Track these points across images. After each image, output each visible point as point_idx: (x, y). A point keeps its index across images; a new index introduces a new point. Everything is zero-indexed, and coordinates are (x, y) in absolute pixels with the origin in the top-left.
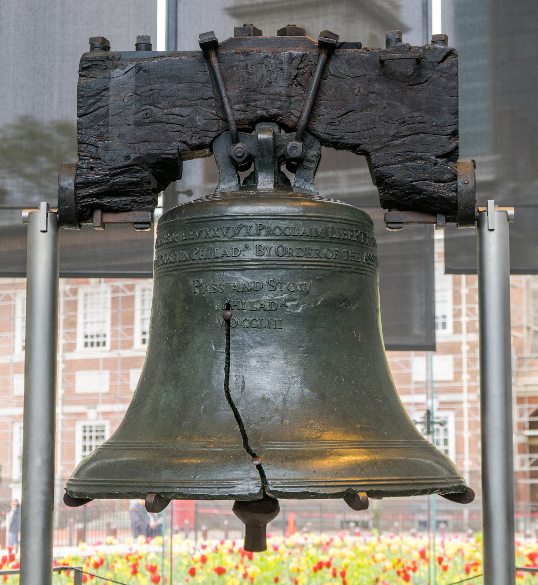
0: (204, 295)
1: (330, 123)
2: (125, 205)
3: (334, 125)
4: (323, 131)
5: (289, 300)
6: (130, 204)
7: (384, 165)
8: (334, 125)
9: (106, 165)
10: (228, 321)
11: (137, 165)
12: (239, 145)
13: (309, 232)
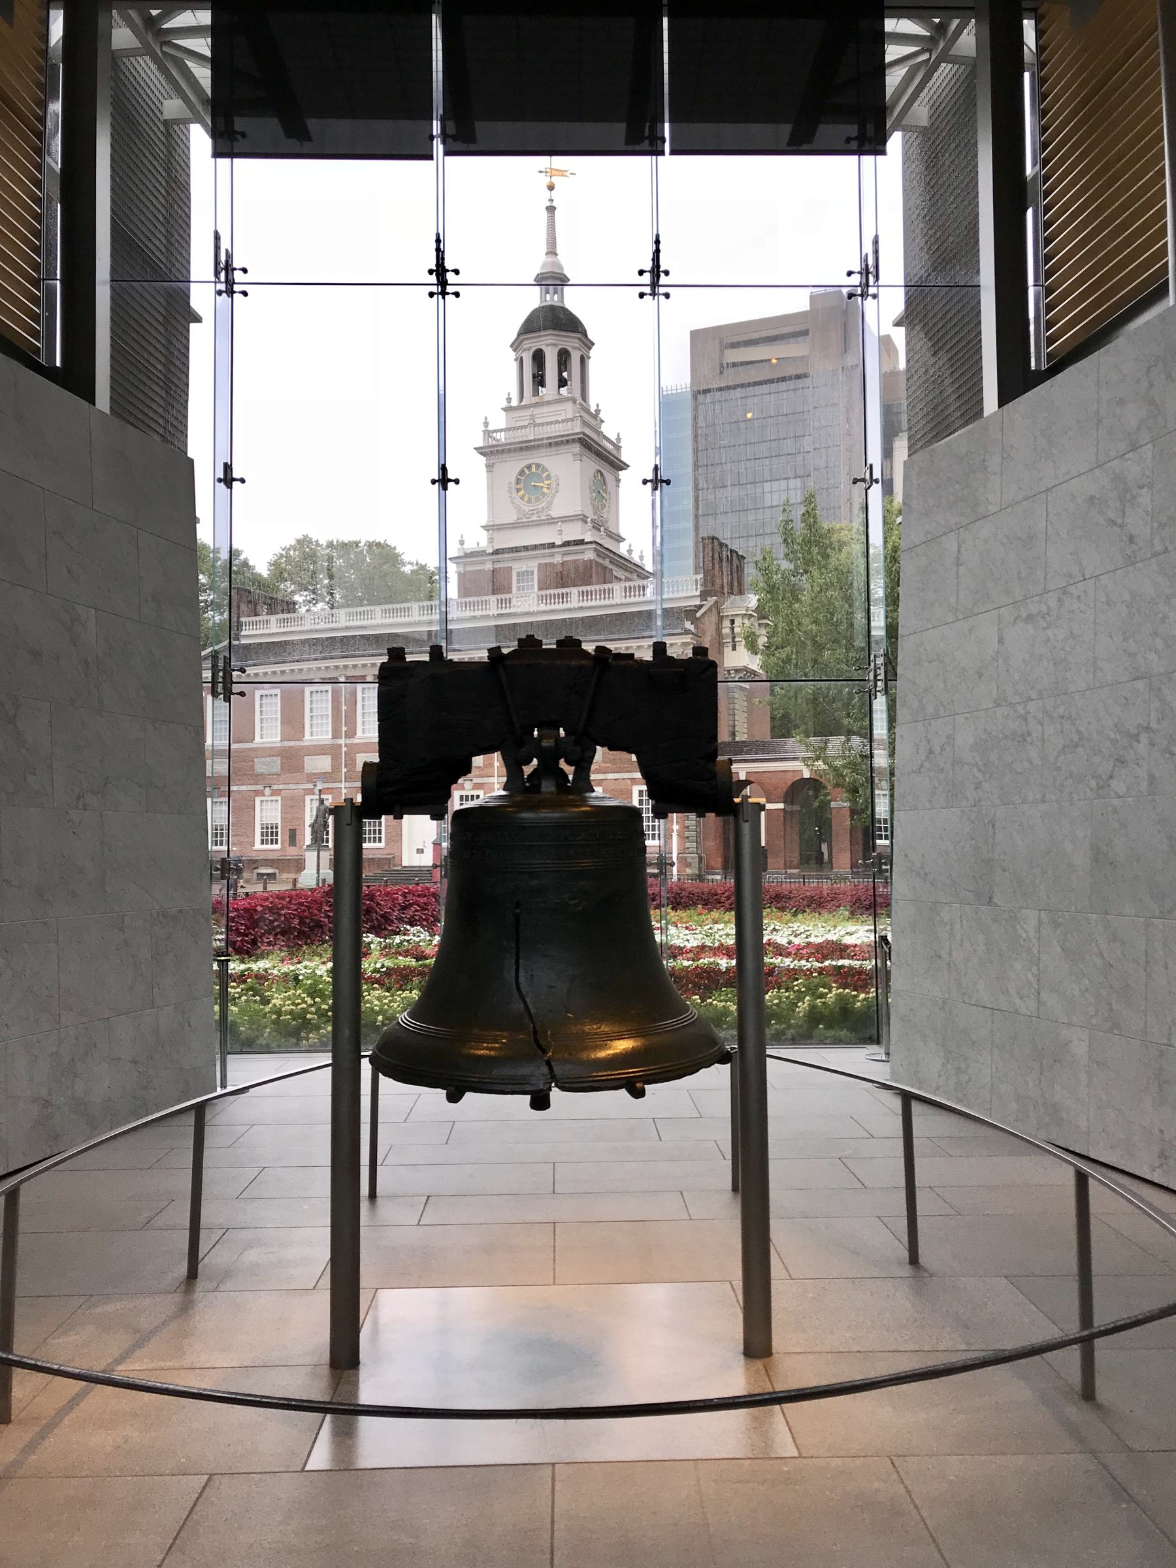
10: (517, 918)
12: (524, 749)
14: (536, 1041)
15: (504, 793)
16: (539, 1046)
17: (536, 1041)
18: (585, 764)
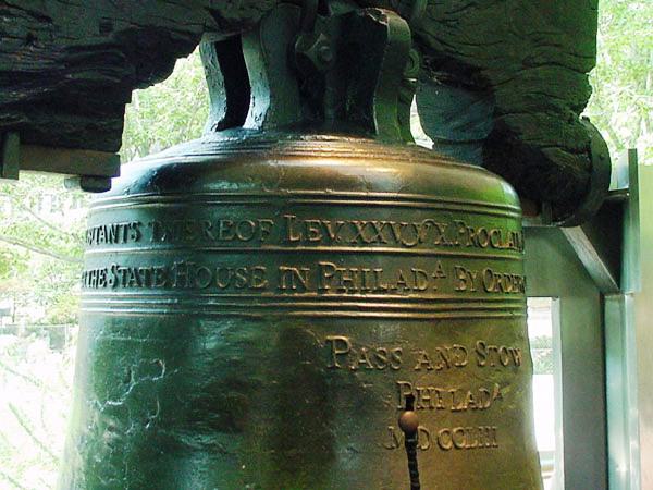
1: (443, 21)
3: (449, 26)
4: (435, 34)
8: (449, 26)
10: (411, 432)
12: (322, 37)
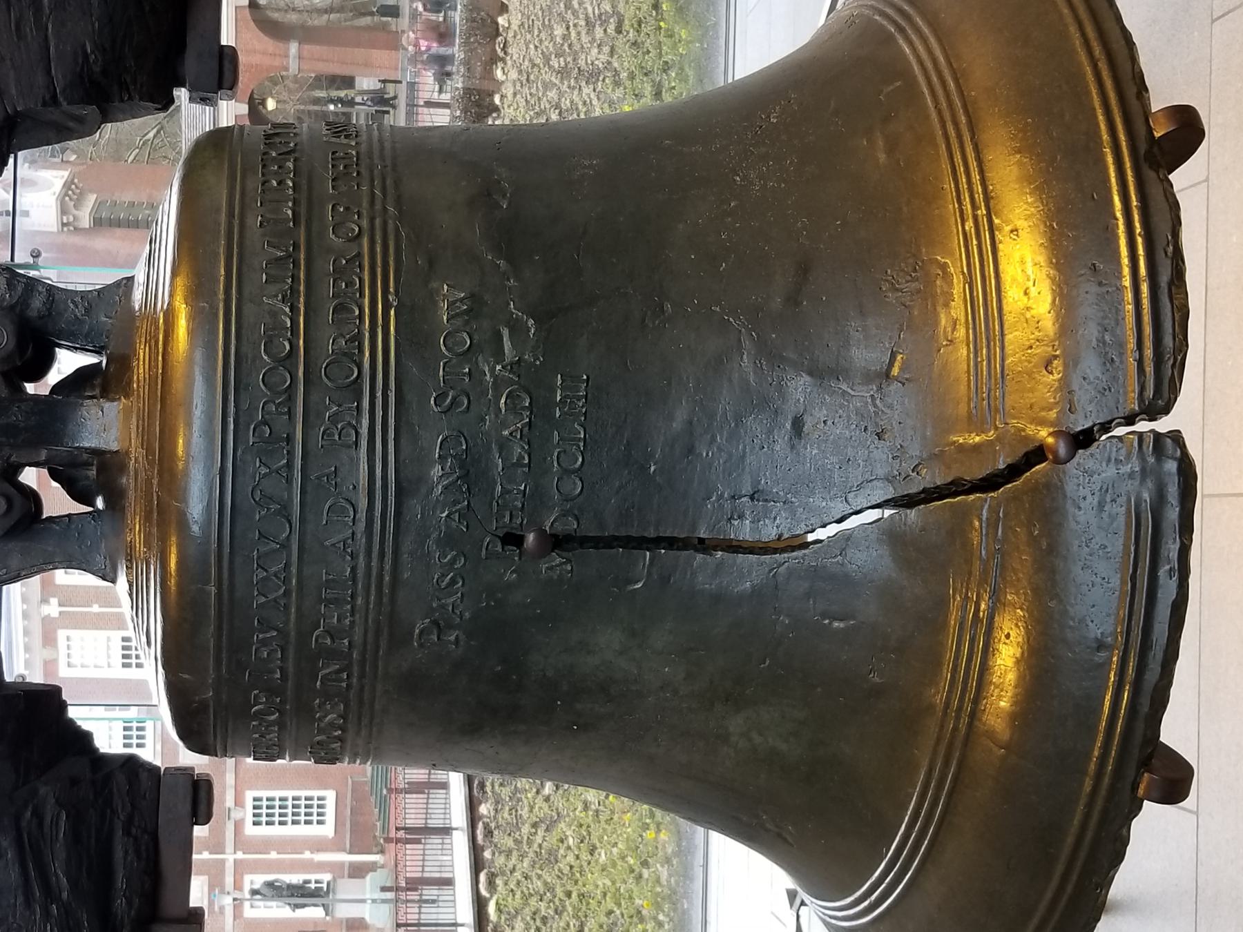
0: (467, 615)
2: (137, 852)
5: (499, 354)
6: (136, 839)
7: (49, 72)
9: (14, 916)
10: (556, 542)
11: (18, 818)
13: (278, 286)
14: (989, 483)
15: (122, 580)
16: (1013, 471)
17: (989, 483)
18: (37, 303)
